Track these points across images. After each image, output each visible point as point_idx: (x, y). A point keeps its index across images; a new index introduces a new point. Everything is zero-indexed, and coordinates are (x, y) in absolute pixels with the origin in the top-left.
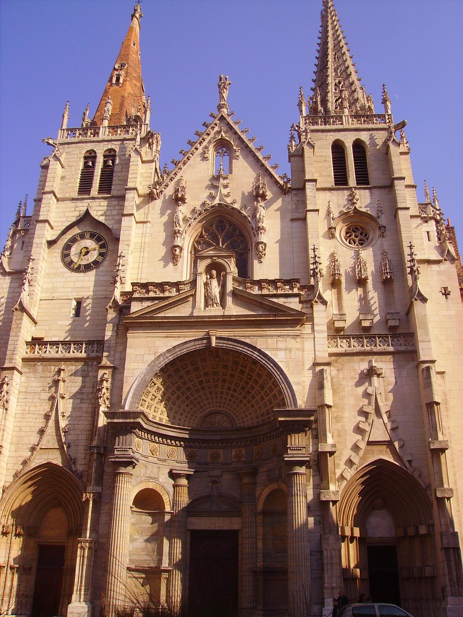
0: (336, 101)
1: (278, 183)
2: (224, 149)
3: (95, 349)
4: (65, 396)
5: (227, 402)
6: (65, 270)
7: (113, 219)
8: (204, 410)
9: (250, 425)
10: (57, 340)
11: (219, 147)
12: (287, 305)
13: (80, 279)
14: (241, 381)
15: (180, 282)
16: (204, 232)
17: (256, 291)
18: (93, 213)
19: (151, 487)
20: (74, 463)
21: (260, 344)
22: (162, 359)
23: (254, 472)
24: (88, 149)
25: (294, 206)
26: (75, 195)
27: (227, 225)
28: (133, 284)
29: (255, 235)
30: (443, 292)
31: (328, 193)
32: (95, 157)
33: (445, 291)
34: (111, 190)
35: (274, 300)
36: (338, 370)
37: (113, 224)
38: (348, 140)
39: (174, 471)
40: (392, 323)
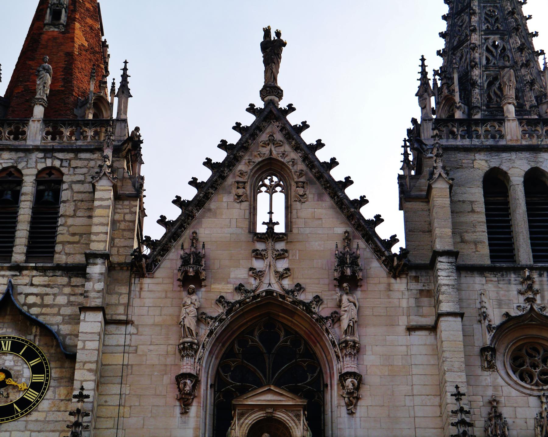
0: (490, 84)
2: (275, 179)
7: (58, 314)
16: (236, 347)
24: (5, 165)
25: (412, 302)
27: (282, 334)
29: (338, 357)
32: (20, 182)
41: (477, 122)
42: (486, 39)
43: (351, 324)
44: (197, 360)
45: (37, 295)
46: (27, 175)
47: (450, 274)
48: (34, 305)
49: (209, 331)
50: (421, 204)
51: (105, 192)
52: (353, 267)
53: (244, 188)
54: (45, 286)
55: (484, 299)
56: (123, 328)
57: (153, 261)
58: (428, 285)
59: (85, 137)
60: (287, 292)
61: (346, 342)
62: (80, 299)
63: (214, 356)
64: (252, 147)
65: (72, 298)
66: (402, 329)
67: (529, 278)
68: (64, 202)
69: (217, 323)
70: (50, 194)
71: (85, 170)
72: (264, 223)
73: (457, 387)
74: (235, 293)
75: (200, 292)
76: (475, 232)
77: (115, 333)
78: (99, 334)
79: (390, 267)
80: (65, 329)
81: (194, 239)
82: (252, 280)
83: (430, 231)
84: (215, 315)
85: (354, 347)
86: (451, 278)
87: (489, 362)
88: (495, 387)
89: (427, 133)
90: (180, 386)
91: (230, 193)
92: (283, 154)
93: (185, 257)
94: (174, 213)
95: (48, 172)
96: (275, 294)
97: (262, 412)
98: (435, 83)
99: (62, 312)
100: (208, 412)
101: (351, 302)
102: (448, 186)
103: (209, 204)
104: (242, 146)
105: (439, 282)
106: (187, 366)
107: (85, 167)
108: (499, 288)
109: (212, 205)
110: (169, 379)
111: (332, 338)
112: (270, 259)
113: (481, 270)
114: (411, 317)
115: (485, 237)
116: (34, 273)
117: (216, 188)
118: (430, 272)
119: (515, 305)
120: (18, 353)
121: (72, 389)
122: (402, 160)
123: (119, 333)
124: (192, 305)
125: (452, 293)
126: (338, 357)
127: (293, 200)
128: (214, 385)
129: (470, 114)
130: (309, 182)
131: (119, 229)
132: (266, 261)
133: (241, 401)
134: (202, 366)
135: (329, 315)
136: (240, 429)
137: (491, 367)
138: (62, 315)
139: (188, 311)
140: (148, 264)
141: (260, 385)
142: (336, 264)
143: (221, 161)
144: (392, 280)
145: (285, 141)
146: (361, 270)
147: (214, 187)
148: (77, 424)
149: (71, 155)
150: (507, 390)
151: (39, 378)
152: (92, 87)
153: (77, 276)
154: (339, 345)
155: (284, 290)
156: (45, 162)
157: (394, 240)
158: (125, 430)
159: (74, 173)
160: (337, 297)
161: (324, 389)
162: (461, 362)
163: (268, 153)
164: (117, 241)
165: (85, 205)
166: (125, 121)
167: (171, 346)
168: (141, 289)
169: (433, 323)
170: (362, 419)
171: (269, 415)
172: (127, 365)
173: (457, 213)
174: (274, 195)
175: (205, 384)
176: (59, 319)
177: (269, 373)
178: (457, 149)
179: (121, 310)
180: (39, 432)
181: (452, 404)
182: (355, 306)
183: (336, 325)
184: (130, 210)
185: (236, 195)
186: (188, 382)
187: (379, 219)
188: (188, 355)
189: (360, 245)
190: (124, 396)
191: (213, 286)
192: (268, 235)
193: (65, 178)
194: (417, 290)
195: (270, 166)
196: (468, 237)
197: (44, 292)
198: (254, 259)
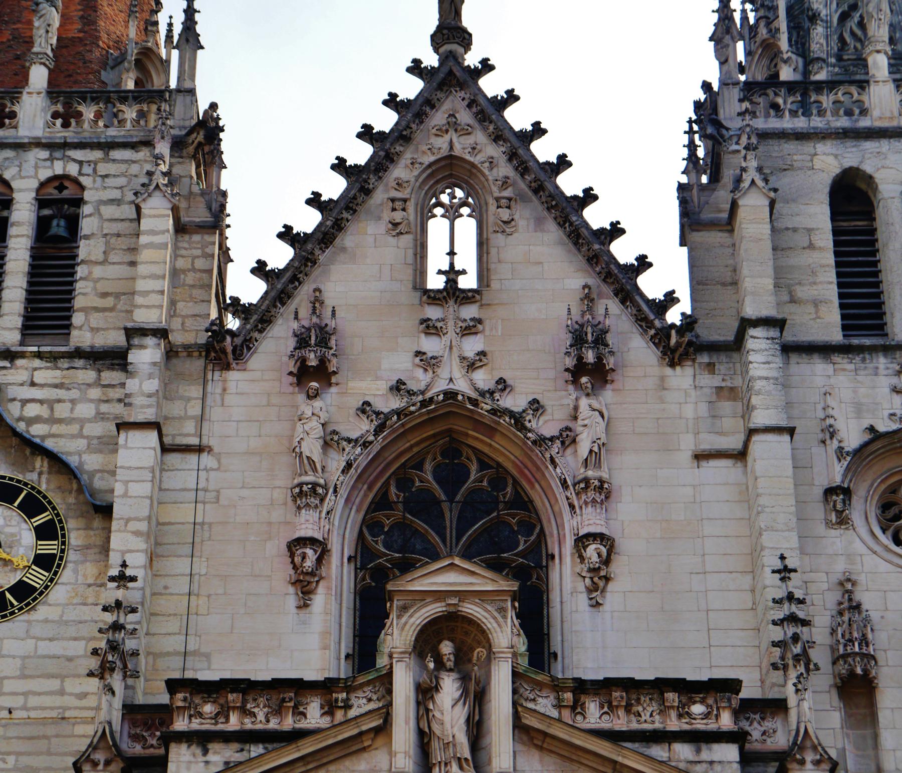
2: (459, 193)
7: (80, 435)
11: (440, 187)
15: (338, 680)
16: (393, 490)
25: (703, 409)
27: (474, 468)
28: (173, 686)
34: (68, 327)
41: (819, 87)
43: (596, 449)
44: (323, 515)
45: (41, 402)
46: (20, 190)
47: (771, 358)
48: (37, 420)
49: (344, 464)
50: (720, 234)
51: (158, 217)
52: (598, 349)
53: (404, 210)
54: (56, 386)
55: (830, 401)
56: (193, 458)
57: (245, 340)
58: (731, 378)
59: (122, 122)
60: (482, 394)
61: (586, 480)
62: (118, 409)
63: (354, 508)
64: (418, 136)
65: (104, 408)
66: (685, 456)
68: (87, 237)
69: (359, 449)
70: (62, 223)
71: (122, 181)
72: (440, 272)
73: (782, 558)
74: (390, 396)
75: (329, 395)
76: (815, 283)
77: (180, 468)
78: (153, 471)
79: (664, 347)
80: (92, 462)
81: (317, 302)
82: (420, 373)
83: (735, 283)
84: (354, 435)
85: (601, 488)
86: (771, 365)
87: (839, 513)
88: (850, 557)
89: (730, 109)
90: (296, 559)
91: (380, 218)
92: (474, 149)
93: (302, 334)
94: (280, 256)
95: (57, 184)
96: (460, 397)
97: (439, 604)
98: (744, 18)
99: (86, 432)
100: (344, 605)
101: (594, 410)
102: (767, 203)
103: (342, 240)
104: (401, 135)
105: (751, 373)
106: (308, 524)
107: (123, 175)
108: (858, 382)
109: (348, 240)
110: (277, 547)
111: (562, 473)
113: (825, 350)
114: (702, 436)
115: (832, 292)
116: (37, 363)
117: (355, 211)
118: (735, 355)
119: (886, 413)
120: (12, 503)
121: (107, 567)
122: (686, 156)
123: (187, 467)
124: (315, 418)
125: (773, 392)
126: (572, 506)
127: (491, 229)
128: (355, 557)
129: (806, 73)
130: (521, 198)
131: (184, 285)
132: (444, 338)
133: (402, 585)
134: (337, 525)
135: (557, 434)
136: (400, 635)
137: (843, 521)
138: (87, 437)
139: (306, 427)
140: (236, 346)
141: (435, 557)
142: (568, 344)
143: (362, 161)
144: (668, 371)
145: (476, 125)
146: (612, 353)
147: (351, 209)
148: (117, 627)
149: (97, 154)
151: (50, 547)
152: (132, 32)
153: (111, 368)
154: (574, 485)
155: (477, 389)
156: (52, 167)
157: (670, 299)
158: (200, 636)
159: (104, 186)
160: (570, 401)
161: (547, 563)
162: (790, 513)
163: (445, 146)
164: (180, 305)
165: (123, 243)
166: (192, 92)
167: (278, 490)
168: (224, 390)
169: (740, 446)
170: (615, 614)
171: (452, 609)
172: (203, 523)
173: (782, 250)
174: (458, 222)
175: (339, 555)
176: (82, 443)
177: (451, 535)
178: (782, 135)
179: (190, 427)
180: (51, 640)
181: (774, 588)
182: (603, 417)
183: (569, 451)
184: (203, 251)
185: (390, 222)
186: (309, 552)
187: (643, 263)
188: (307, 505)
189: (611, 311)
190: (196, 578)
191: (351, 384)
192: (448, 293)
193: (87, 195)
194: (711, 387)
195: (450, 171)
196: (802, 292)
197: (54, 397)
198: (423, 335)
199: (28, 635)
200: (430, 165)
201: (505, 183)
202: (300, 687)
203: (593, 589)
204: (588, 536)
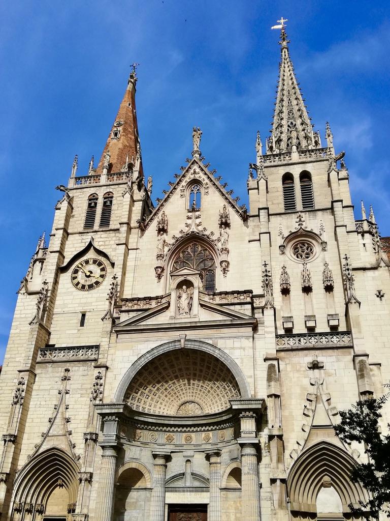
1: (239, 212)
3: (94, 352)
4: (68, 392)
5: (198, 392)
6: (74, 289)
8: (179, 399)
9: (217, 412)
10: (65, 346)
12: (241, 311)
13: (85, 296)
14: (208, 375)
17: (218, 300)
18: (96, 244)
19: (133, 467)
20: (74, 447)
21: (220, 344)
22: (143, 359)
23: (218, 454)
26: (81, 229)
30: (378, 294)
31: (278, 218)
32: (97, 199)
33: (380, 293)
35: (232, 308)
36: (286, 364)
37: (111, 252)
38: (296, 171)
39: (153, 453)
40: (333, 323)
42: (288, 122)
48: (102, 245)
54: (106, 238)
67: (300, 216)
91: (178, 194)
106: (160, 263)
112: (193, 218)
137: (283, 253)
149: (117, 186)
150: (290, 262)
151: (103, 273)
179: (135, 244)
186: (159, 269)
193: (114, 196)
199: (98, 293)
200: (190, 181)
201: (207, 184)
202: (150, 299)
203: (224, 273)
204: (222, 261)
